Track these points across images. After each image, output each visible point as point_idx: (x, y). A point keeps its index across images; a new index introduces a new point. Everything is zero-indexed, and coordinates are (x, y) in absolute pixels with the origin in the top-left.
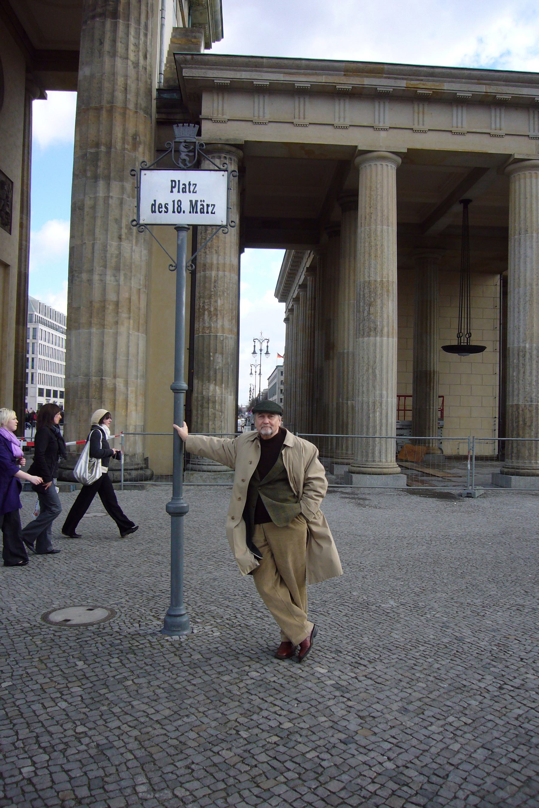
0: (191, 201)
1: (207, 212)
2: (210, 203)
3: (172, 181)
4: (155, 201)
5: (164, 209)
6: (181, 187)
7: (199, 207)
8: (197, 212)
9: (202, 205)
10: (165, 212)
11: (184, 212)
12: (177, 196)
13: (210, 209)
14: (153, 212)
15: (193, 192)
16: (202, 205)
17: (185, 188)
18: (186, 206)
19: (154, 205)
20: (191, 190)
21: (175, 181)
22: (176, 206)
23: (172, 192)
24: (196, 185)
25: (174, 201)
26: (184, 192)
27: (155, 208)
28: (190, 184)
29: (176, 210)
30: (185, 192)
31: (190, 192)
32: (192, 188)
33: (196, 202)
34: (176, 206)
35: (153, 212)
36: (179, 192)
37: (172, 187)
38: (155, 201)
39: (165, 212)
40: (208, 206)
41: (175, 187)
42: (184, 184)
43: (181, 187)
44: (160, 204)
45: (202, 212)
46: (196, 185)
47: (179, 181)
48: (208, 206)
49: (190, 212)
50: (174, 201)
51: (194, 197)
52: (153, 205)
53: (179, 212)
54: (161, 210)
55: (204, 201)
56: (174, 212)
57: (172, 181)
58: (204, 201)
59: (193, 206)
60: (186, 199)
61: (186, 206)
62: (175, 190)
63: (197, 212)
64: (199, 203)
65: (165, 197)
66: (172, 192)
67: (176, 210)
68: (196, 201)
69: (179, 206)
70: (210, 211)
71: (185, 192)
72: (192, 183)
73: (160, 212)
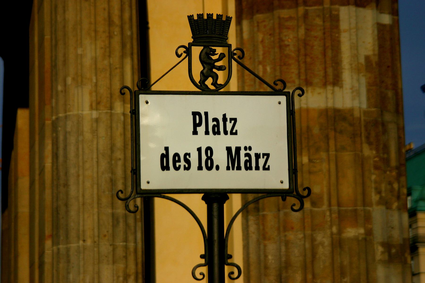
0: (229, 149)
1: (257, 168)
2: (261, 151)
3: (195, 114)
4: (167, 149)
5: (183, 163)
6: (211, 124)
7: (243, 159)
8: (239, 168)
9: (247, 155)
11: (218, 168)
12: (204, 140)
13: (262, 161)
14: (165, 168)
15: (232, 133)
17: (218, 126)
18: (220, 158)
19: (164, 156)
20: (229, 129)
21: (199, 114)
22: (204, 157)
23: (195, 132)
24: (235, 120)
25: (199, 150)
26: (216, 132)
28: (225, 119)
31: (226, 133)
32: (229, 126)
33: (238, 149)
34: (204, 157)
35: (165, 168)
36: (207, 133)
37: (196, 125)
38: (167, 149)
40: (257, 156)
41: (200, 124)
42: (215, 120)
43: (211, 124)
44: (176, 155)
45: (248, 168)
46: (235, 120)
47: (206, 114)
48: (257, 156)
49: (228, 168)
50: (199, 150)
51: (233, 142)
52: (163, 156)
53: (209, 168)
54: (178, 164)
56: (200, 168)
57: (195, 114)
58: (250, 149)
59: (233, 156)
60: (220, 144)
61: (220, 158)
62: (201, 130)
63: (239, 168)
64: (243, 152)
66: (195, 132)
68: (238, 149)
69: (210, 158)
70: (261, 164)
72: (228, 117)
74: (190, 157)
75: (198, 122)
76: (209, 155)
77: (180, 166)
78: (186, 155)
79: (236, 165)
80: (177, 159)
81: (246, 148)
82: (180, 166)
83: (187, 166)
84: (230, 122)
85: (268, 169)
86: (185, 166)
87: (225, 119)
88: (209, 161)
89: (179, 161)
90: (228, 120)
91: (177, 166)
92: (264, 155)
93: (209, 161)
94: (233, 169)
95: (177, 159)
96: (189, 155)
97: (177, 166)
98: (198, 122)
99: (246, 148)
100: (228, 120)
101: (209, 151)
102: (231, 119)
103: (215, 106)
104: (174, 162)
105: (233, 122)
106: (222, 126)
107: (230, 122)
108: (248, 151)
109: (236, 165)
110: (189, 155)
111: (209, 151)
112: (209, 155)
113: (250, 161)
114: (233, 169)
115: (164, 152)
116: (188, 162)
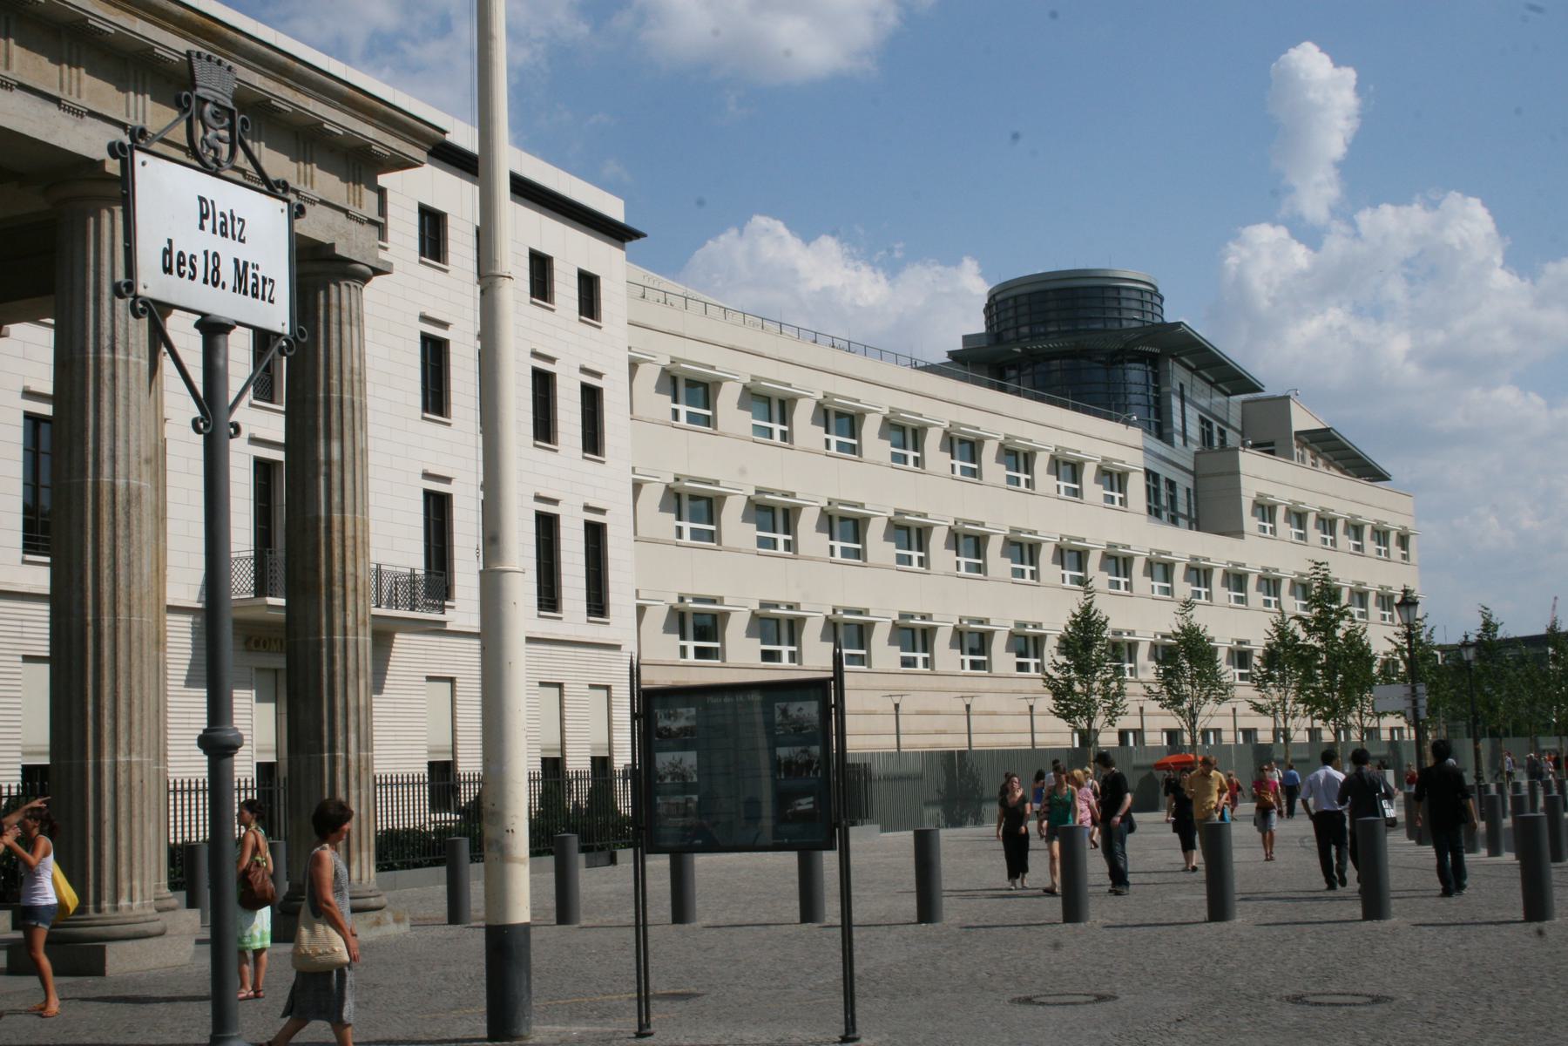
2: (268, 277)
4: (170, 241)
5: (187, 269)
6: (219, 220)
7: (251, 281)
8: (245, 293)
9: (255, 276)
16: (255, 276)
18: (228, 273)
19: (167, 252)
23: (202, 227)
25: (206, 253)
27: (173, 262)
32: (238, 227)
37: (204, 216)
38: (170, 241)
40: (264, 280)
43: (219, 220)
44: (181, 254)
50: (206, 253)
51: (244, 253)
56: (205, 281)
60: (229, 251)
62: (208, 223)
64: (250, 271)
66: (202, 227)
69: (216, 269)
72: (236, 216)
73: (181, 275)
87: (233, 218)
104: (180, 264)
106: (228, 227)
116: (193, 267)
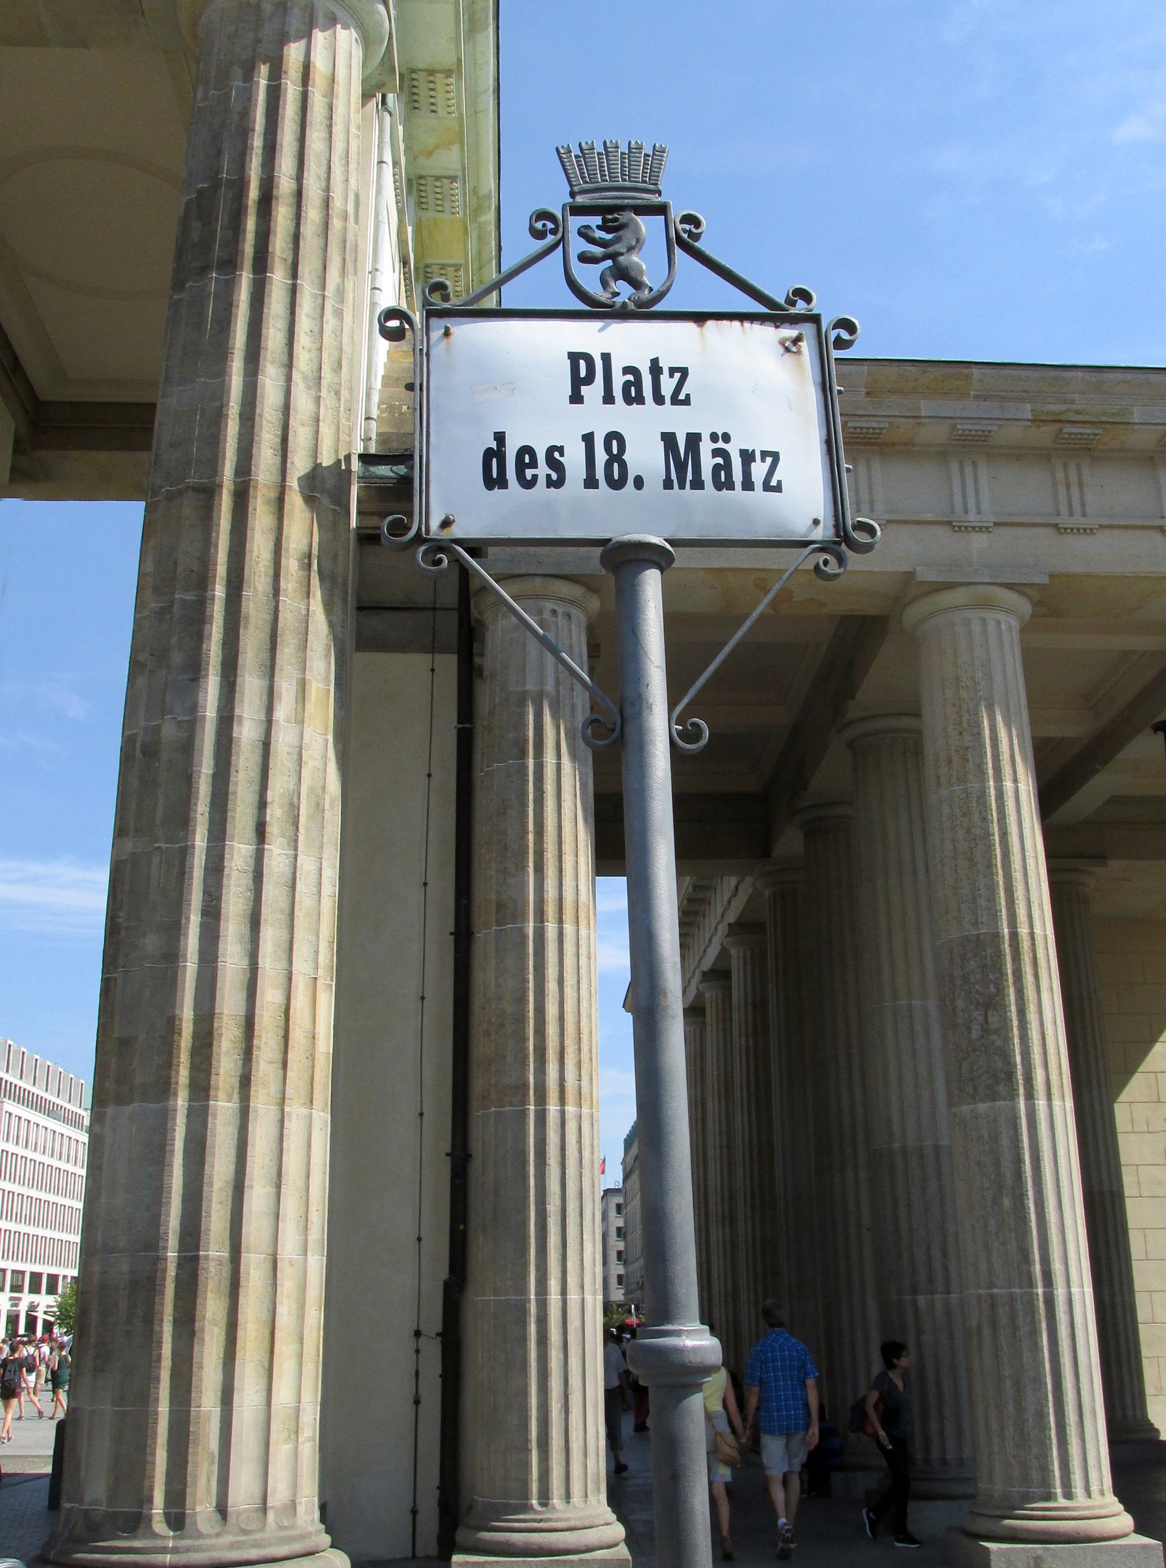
0: (669, 439)
1: (748, 485)
3: (574, 357)
4: (500, 437)
5: (543, 470)
6: (619, 380)
7: (708, 462)
8: (698, 484)
9: (716, 453)
10: (550, 483)
11: (639, 483)
12: (598, 416)
13: (759, 470)
15: (675, 401)
17: (638, 383)
18: (647, 456)
19: (494, 455)
21: (588, 358)
22: (601, 457)
25: (588, 439)
26: (633, 396)
28: (655, 368)
29: (600, 473)
30: (640, 400)
31: (659, 399)
33: (693, 440)
34: (601, 457)
36: (609, 399)
37: (578, 382)
39: (550, 483)
41: (590, 379)
43: (619, 380)
44: (526, 450)
46: (684, 372)
47: (606, 358)
48: (747, 457)
49: (668, 484)
50: (588, 439)
51: (681, 422)
52: (489, 454)
53: (617, 484)
54: (529, 473)
55: (726, 438)
56: (591, 482)
57: (574, 357)
58: (726, 438)
59: (681, 456)
61: (647, 456)
62: (593, 392)
63: (698, 484)
65: (550, 422)
67: (600, 473)
68: (693, 440)
69: (616, 459)
71: (640, 400)
72: (665, 364)
74: (562, 455)
75: (583, 374)
76: (615, 451)
77: (535, 477)
78: (551, 450)
79: (689, 476)
80: (527, 460)
81: (714, 437)
82: (535, 477)
83: (554, 476)
84: (671, 376)
85: (778, 488)
86: (548, 476)
87: (655, 368)
88: (616, 465)
89: (534, 464)
90: (666, 372)
91: (529, 477)
92: (764, 454)
93: (616, 465)
94: (682, 486)
95: (527, 460)
96: (561, 450)
97: (529, 477)
98: (583, 374)
99: (714, 437)
100: (666, 372)
101: (615, 443)
102: (672, 371)
103: (629, 343)
104: (521, 467)
105: (677, 375)
107: (671, 376)
108: (721, 444)
109: (689, 476)
110: (561, 450)
111: (615, 443)
112: (615, 451)
113: (727, 466)
114: (682, 486)
115: (494, 445)
116: (555, 464)
